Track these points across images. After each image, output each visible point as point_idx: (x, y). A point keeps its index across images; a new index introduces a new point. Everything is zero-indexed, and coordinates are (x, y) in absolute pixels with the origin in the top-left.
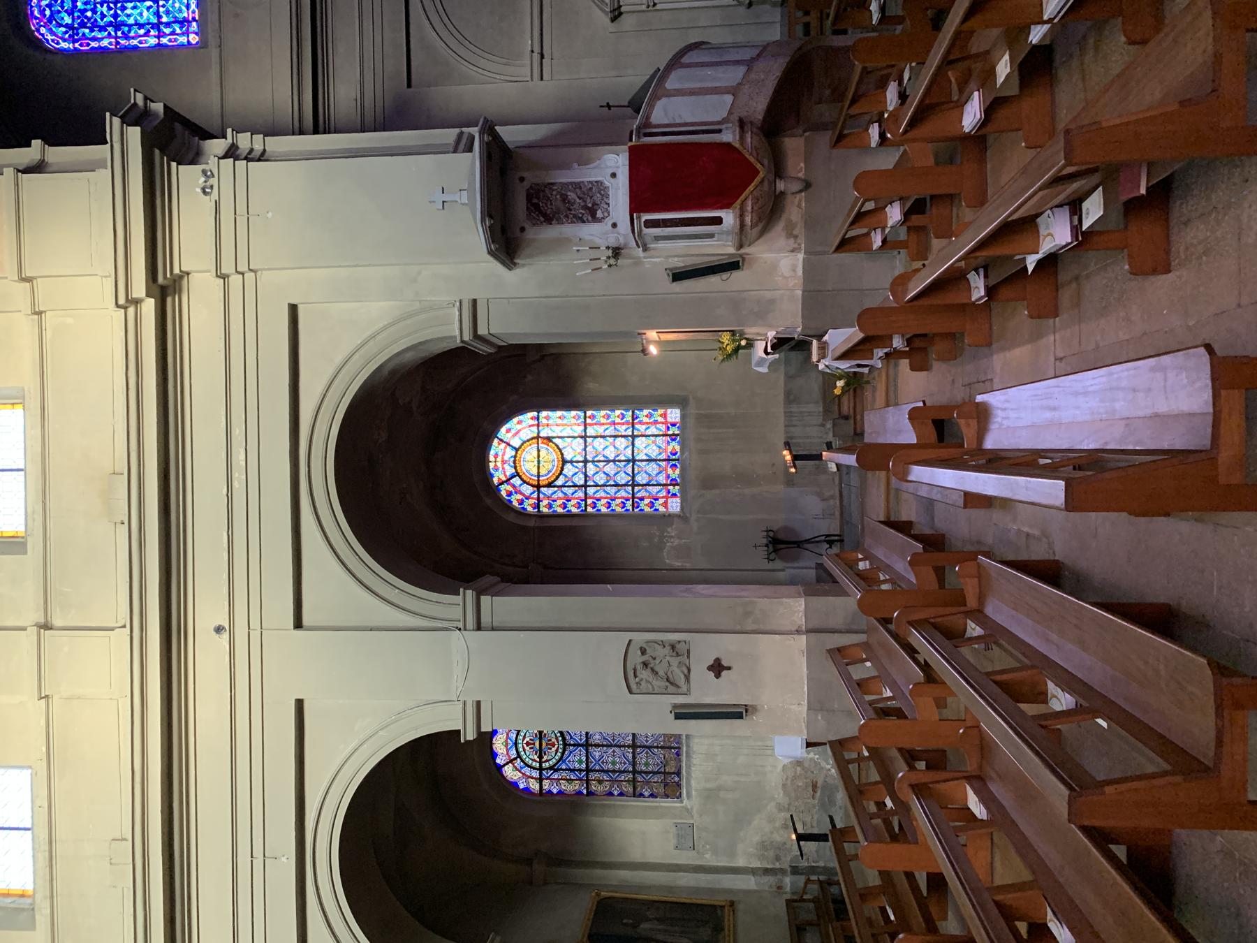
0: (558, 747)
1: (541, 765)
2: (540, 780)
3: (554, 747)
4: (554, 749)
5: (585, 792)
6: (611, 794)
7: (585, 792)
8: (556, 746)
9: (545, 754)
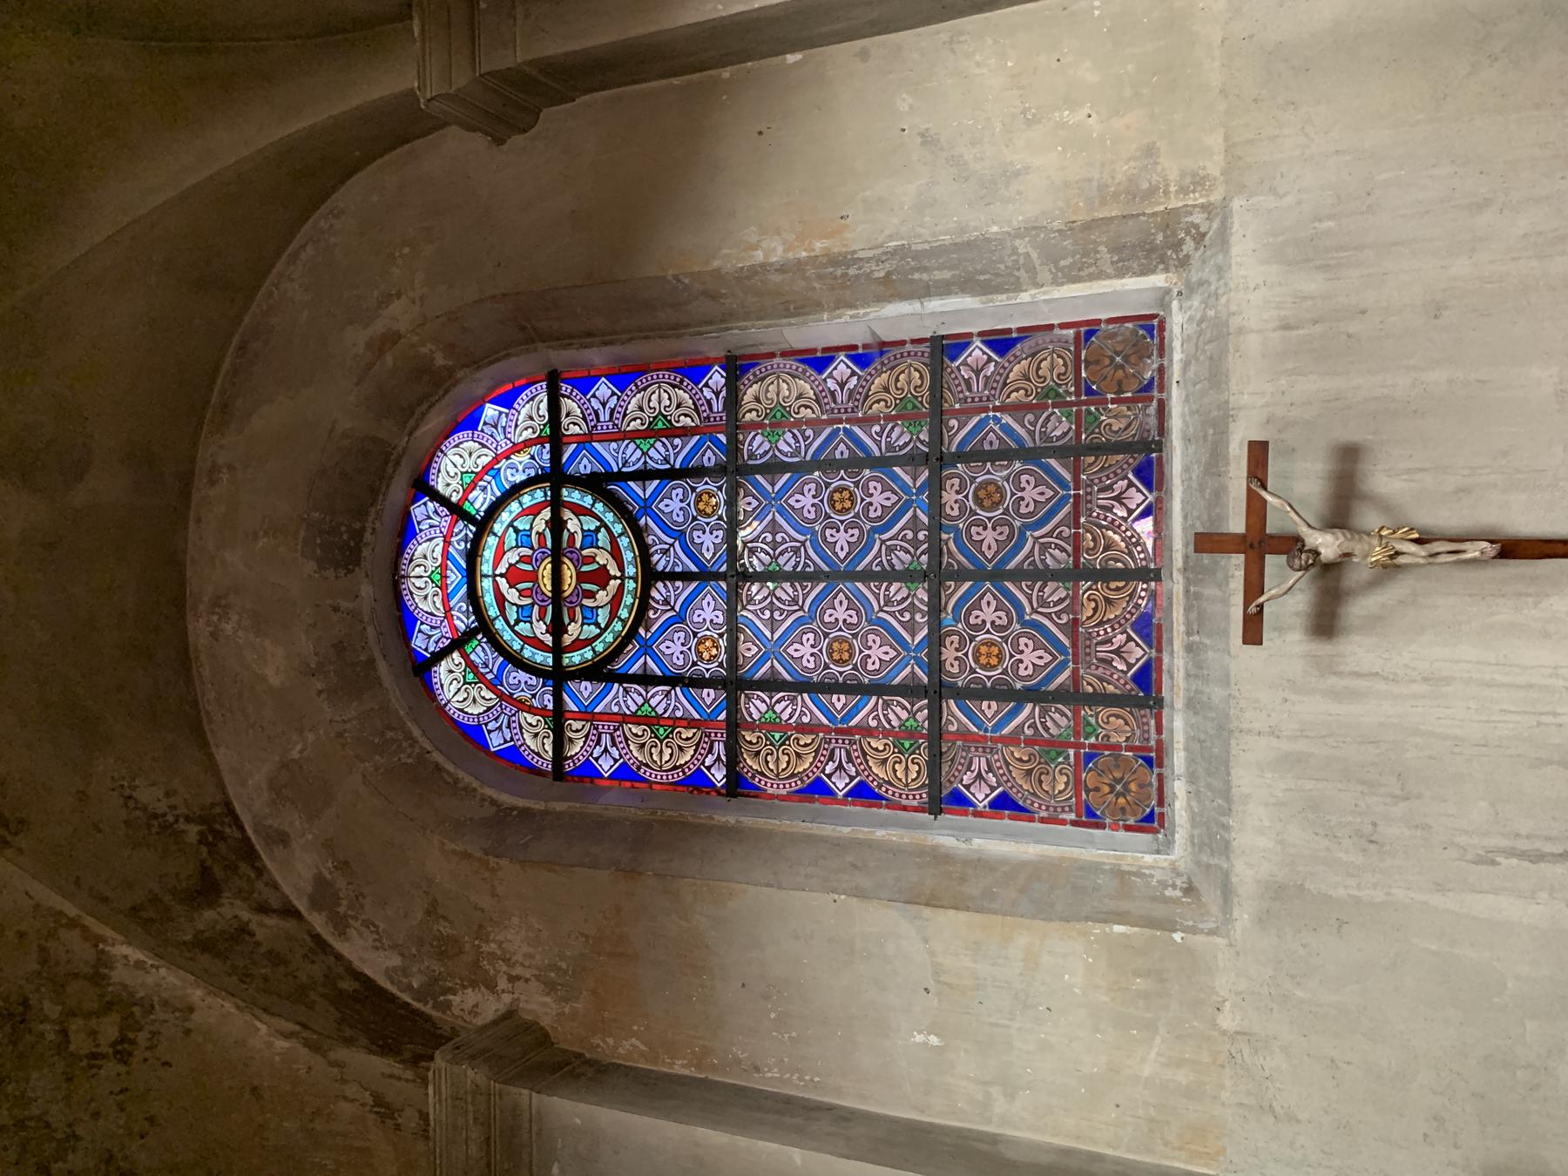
0: (621, 587)
1: (557, 659)
2: (557, 719)
3: (604, 588)
4: (603, 597)
5: (718, 776)
6: (819, 789)
7: (718, 776)
8: (614, 584)
9: (572, 620)
